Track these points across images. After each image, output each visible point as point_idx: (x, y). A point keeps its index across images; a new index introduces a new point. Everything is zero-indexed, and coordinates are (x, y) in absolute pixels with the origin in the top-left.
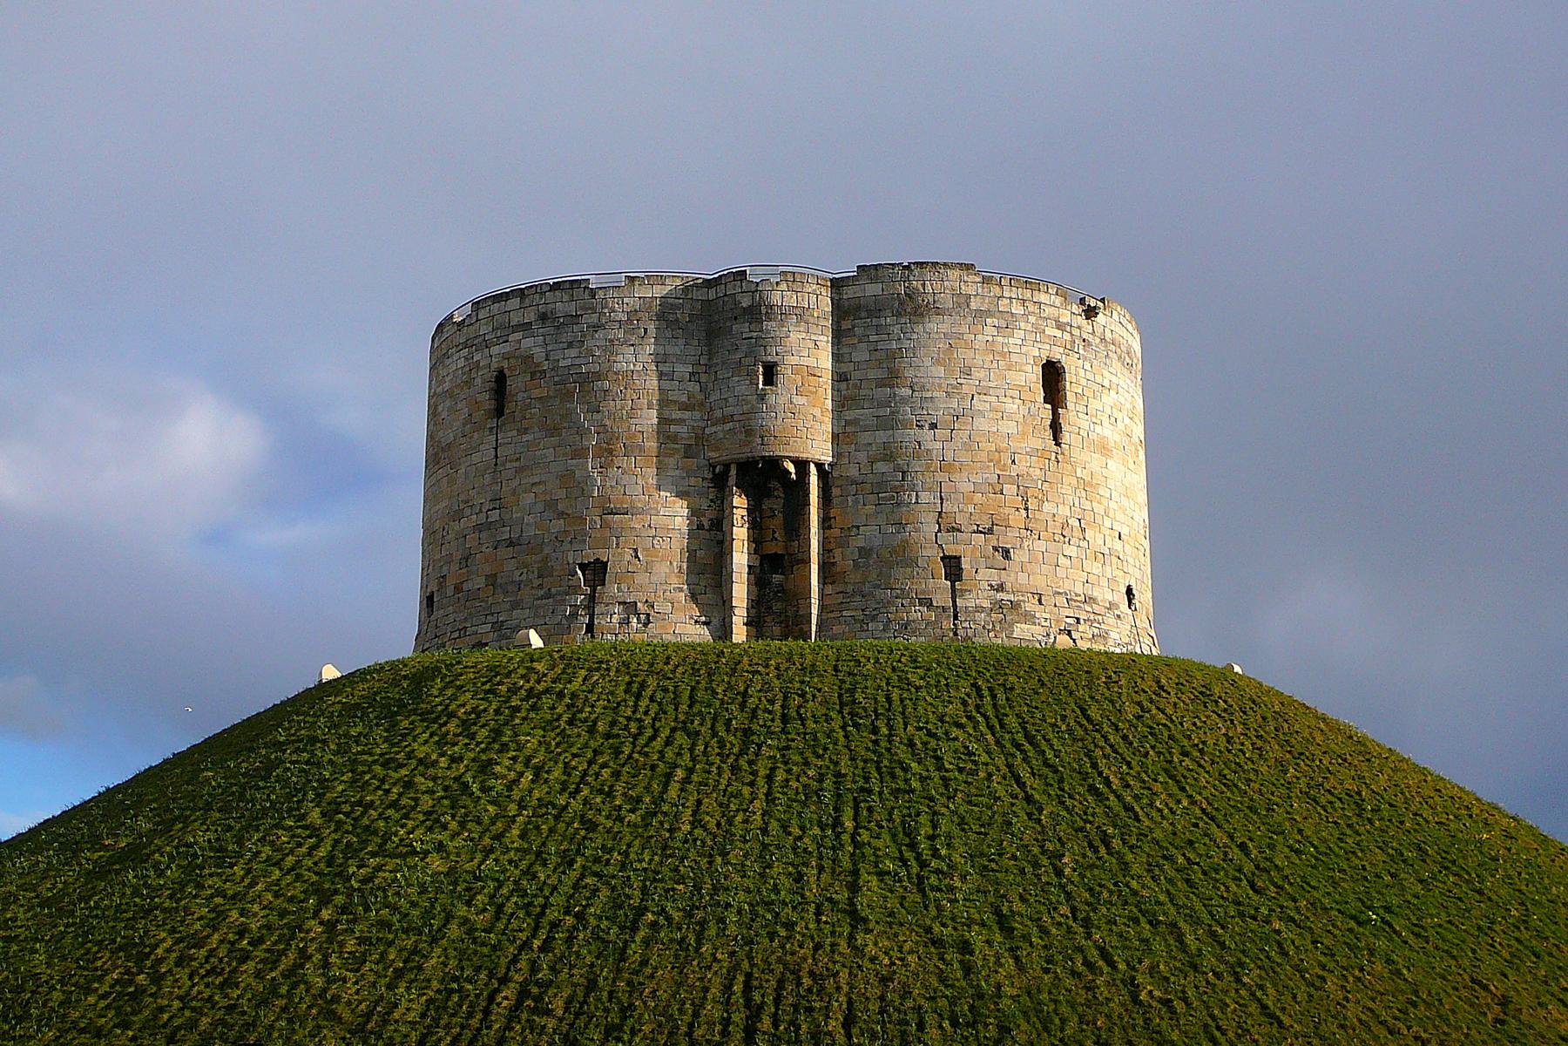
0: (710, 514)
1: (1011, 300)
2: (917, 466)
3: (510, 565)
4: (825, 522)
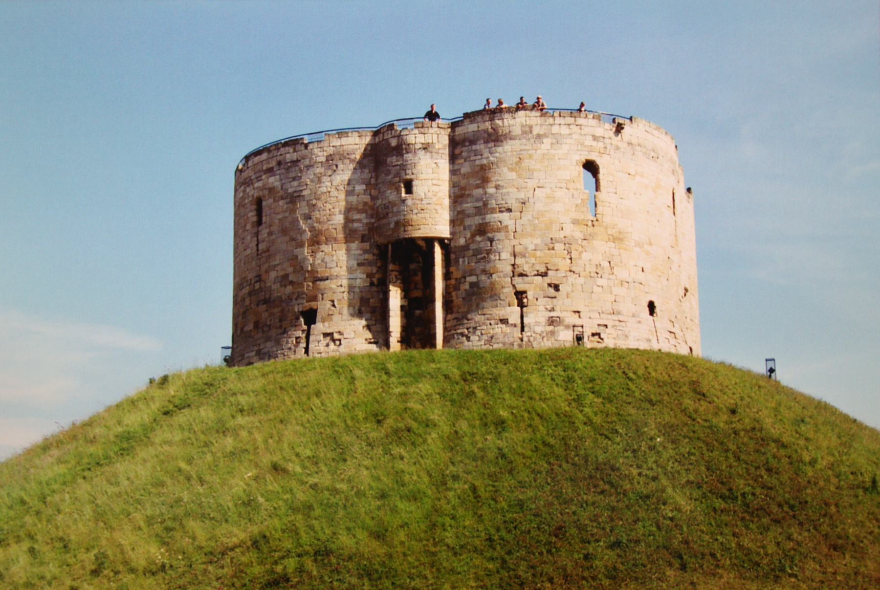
0: (377, 276)
1: (560, 126)
2: (498, 236)
3: (265, 315)
4: (447, 276)
